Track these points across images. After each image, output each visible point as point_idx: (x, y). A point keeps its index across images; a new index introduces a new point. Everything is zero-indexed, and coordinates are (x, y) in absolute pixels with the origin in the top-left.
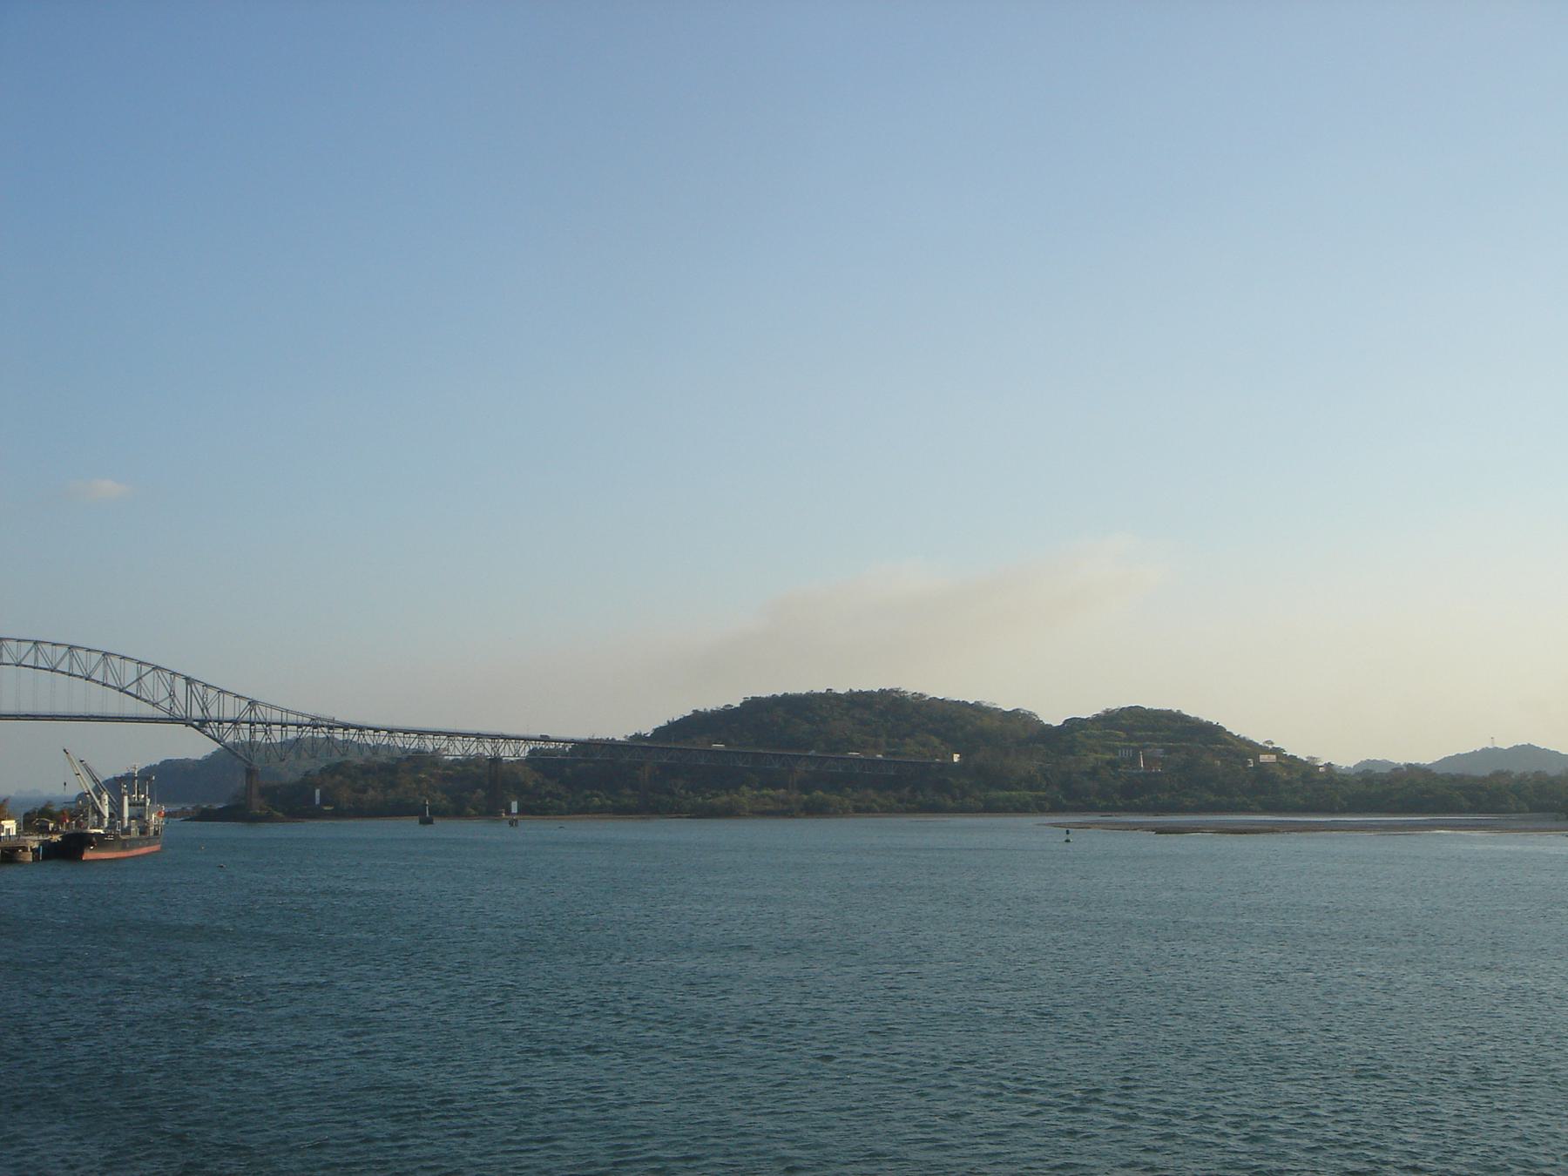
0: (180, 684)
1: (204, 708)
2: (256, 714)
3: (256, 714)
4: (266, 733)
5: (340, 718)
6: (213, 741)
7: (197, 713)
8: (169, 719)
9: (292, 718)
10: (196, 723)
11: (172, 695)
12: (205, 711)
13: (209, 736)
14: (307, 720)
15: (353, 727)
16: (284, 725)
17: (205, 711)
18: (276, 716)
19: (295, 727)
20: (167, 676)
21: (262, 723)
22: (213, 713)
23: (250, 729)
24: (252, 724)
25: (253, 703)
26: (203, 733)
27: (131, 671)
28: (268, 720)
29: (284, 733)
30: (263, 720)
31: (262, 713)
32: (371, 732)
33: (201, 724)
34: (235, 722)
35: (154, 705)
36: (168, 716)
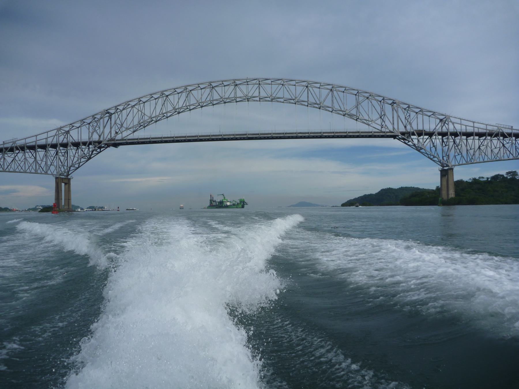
33: (405, 136)
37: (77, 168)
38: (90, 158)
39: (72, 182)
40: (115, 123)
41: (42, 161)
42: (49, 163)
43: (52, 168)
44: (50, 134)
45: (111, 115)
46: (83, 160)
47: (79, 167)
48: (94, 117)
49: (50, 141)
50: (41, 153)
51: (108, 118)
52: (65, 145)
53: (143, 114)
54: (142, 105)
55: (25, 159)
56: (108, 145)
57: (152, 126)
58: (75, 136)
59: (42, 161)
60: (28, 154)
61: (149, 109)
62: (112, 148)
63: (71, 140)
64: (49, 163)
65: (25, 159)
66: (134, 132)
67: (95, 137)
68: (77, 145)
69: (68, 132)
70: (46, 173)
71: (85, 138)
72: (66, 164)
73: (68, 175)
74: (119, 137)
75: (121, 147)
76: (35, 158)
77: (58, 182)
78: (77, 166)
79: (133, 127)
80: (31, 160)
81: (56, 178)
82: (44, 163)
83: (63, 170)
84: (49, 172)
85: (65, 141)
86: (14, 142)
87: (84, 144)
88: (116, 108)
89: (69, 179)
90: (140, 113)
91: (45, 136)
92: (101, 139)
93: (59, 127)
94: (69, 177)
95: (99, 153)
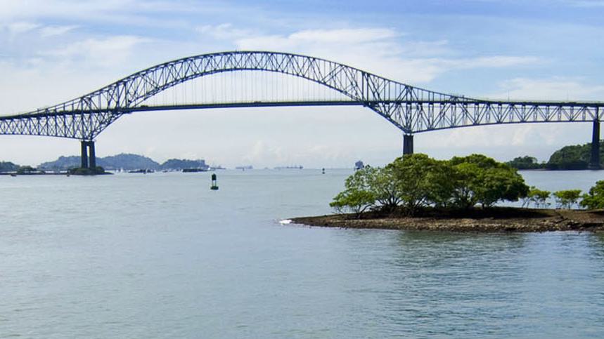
2: (411, 96)
3: (411, 96)
4: (418, 108)
6: (380, 115)
7: (371, 98)
9: (437, 98)
12: (376, 94)
13: (381, 113)
14: (448, 98)
15: (505, 103)
16: (431, 103)
17: (376, 94)
18: (425, 96)
20: (350, 69)
21: (416, 102)
23: (407, 107)
24: (409, 103)
25: (409, 89)
26: (376, 110)
27: (325, 70)
28: (420, 99)
29: (431, 109)
30: (416, 99)
32: (497, 105)
33: (372, 105)
34: (398, 103)
35: (346, 93)
37: (99, 133)
38: (109, 123)
39: (96, 145)
41: (70, 126)
42: (76, 128)
43: (78, 133)
44: (75, 101)
45: (125, 84)
46: (102, 125)
47: (101, 131)
48: (110, 86)
49: (75, 108)
50: (69, 118)
51: (123, 85)
53: (152, 83)
54: (150, 75)
55: (56, 123)
56: (124, 113)
57: (160, 94)
58: (97, 103)
59: (70, 126)
60: (59, 119)
61: (159, 78)
62: (125, 115)
63: (93, 107)
64: (76, 128)
65: (56, 123)
66: (145, 99)
67: (113, 105)
68: (99, 111)
69: (90, 99)
70: (74, 137)
71: (104, 106)
72: (89, 129)
73: (92, 138)
74: (132, 105)
75: (134, 113)
76: (65, 123)
77: (84, 145)
78: (99, 131)
79: (144, 95)
80: (61, 125)
81: (82, 143)
82: (71, 127)
83: (87, 134)
84: (76, 136)
85: (88, 109)
86: (47, 109)
87: (104, 111)
88: (129, 78)
89: (93, 143)
90: (148, 84)
91: (72, 103)
93: (82, 96)
94: (93, 140)
95: (116, 118)
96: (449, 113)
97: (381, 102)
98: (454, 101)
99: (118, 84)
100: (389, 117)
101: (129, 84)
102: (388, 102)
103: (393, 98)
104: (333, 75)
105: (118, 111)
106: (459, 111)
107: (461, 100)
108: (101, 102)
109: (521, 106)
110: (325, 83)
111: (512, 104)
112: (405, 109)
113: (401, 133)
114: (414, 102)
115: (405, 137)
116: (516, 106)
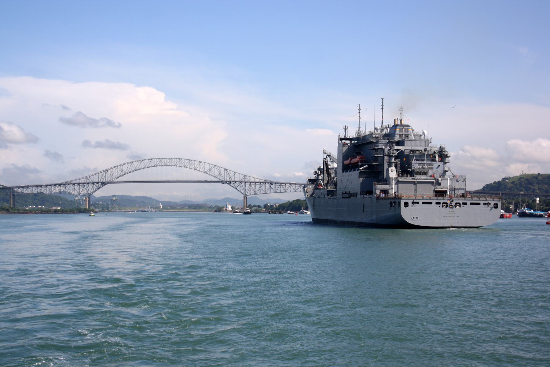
0: (223, 171)
1: (230, 178)
5: (273, 180)
7: (228, 179)
8: (218, 181)
9: (258, 180)
10: (228, 183)
11: (220, 174)
18: (253, 180)
19: (259, 183)
20: (219, 168)
22: (233, 180)
24: (246, 182)
25: (245, 176)
27: (207, 167)
28: (250, 181)
31: (248, 179)
33: (230, 183)
35: (216, 177)
36: (218, 180)
40: (110, 175)
52: (88, 183)
61: (125, 168)
68: (93, 183)
85: (88, 181)
92: (104, 181)
96: (263, 187)
97: (233, 182)
98: (265, 182)
99: (105, 171)
100: (236, 188)
101: (109, 171)
102: (236, 182)
103: (238, 180)
104: (210, 169)
105: (104, 184)
106: (268, 186)
107: (268, 182)
108: (94, 179)
109: (294, 185)
110: (206, 173)
111: (291, 184)
112: (244, 185)
113: (243, 195)
114: (247, 182)
115: (244, 197)
116: (292, 185)
